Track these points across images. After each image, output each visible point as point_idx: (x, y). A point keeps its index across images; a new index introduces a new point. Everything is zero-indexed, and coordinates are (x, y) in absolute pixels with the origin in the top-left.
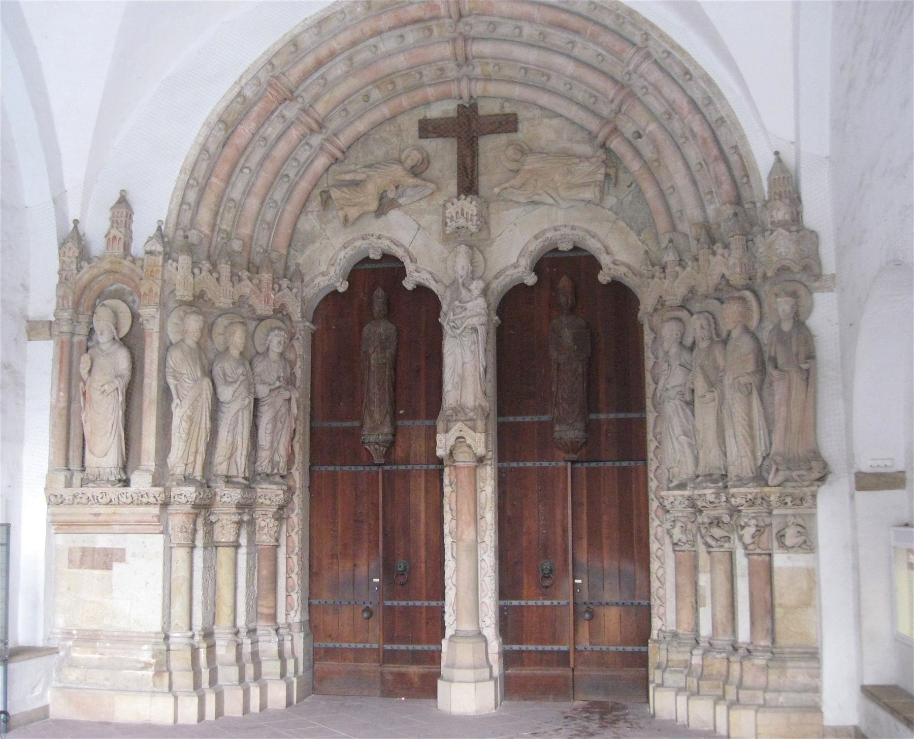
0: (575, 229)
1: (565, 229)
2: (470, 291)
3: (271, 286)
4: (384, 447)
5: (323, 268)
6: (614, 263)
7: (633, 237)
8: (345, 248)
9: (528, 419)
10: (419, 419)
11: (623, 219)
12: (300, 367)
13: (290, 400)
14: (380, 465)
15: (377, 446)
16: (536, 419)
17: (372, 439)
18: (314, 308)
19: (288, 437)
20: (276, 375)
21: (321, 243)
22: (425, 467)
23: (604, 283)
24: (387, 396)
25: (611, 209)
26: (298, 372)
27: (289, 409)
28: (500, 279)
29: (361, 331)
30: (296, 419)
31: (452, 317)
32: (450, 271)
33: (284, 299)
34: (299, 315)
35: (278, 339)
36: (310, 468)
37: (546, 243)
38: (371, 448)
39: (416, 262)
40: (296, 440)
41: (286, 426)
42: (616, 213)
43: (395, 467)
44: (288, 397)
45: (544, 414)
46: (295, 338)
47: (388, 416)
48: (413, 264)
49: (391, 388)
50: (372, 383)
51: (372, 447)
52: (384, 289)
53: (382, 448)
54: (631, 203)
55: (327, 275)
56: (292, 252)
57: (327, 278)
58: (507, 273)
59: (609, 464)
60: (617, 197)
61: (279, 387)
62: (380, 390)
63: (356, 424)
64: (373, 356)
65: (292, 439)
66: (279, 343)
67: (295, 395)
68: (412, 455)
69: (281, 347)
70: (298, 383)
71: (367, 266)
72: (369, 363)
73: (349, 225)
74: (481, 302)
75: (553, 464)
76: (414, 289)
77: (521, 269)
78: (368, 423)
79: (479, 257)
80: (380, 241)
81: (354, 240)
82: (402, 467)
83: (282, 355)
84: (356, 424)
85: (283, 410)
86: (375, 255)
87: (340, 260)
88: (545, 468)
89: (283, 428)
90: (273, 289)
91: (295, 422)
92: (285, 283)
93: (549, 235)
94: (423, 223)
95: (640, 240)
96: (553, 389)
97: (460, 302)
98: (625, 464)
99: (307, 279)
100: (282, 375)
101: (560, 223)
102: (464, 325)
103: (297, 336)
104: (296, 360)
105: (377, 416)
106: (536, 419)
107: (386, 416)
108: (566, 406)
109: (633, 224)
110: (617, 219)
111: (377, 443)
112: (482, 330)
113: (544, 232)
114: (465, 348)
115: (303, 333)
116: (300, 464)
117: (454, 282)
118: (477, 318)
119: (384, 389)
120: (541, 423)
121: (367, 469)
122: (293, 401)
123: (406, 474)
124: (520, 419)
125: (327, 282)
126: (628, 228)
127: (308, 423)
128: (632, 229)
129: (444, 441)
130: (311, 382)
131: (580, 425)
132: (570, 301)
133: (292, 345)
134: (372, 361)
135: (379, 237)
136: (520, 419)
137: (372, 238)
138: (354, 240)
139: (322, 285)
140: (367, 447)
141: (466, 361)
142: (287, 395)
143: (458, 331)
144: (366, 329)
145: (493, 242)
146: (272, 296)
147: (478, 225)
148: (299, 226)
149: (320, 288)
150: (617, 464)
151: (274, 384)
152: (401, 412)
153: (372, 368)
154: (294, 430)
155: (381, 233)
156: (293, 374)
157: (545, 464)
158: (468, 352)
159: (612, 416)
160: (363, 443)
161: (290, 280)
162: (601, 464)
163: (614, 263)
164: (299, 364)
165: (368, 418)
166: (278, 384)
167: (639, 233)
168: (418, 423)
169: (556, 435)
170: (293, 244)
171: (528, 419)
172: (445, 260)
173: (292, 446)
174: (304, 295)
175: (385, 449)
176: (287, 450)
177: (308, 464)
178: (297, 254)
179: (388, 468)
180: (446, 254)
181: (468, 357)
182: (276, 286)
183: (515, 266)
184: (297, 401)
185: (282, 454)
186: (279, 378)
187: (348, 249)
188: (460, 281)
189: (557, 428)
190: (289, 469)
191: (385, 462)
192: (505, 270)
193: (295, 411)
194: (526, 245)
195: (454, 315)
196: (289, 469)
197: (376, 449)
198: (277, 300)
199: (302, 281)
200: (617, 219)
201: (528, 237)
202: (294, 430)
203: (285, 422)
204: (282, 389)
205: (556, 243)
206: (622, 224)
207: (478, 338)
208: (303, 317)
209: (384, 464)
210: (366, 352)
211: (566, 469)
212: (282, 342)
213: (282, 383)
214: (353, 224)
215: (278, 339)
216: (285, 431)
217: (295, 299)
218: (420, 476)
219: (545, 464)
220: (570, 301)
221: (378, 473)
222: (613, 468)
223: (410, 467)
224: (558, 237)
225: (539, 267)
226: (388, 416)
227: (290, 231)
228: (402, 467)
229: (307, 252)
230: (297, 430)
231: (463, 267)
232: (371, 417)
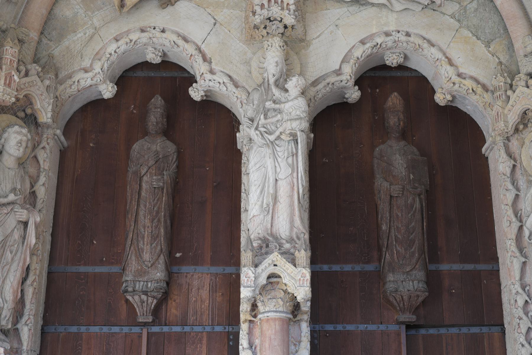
0: (410, 36)
1: (398, 35)
2: (286, 91)
3: (15, 65)
4: (154, 297)
5: (86, 63)
6: (459, 75)
7: (480, 48)
8: (117, 41)
9: (348, 268)
10: (202, 265)
11: (468, 28)
12: (44, 184)
13: (26, 224)
14: (145, 324)
15: (144, 297)
16: (358, 268)
17: (139, 286)
18: (68, 119)
19: (18, 274)
20: (9, 187)
21: (85, 34)
22: (208, 329)
23: (442, 103)
24: (162, 230)
25: (453, 16)
26: (41, 192)
27: (24, 238)
28: (320, 86)
29: (129, 148)
30: (32, 254)
31: (262, 121)
32: (255, 73)
33: (32, 89)
34: (49, 115)
35: (19, 137)
36: (42, 329)
37: (375, 50)
38: (135, 300)
39: (210, 63)
40: (29, 282)
41: (17, 258)
42: (459, 21)
43: (166, 329)
44: (24, 218)
45: (368, 262)
46: (42, 146)
47: (162, 256)
48: (206, 64)
49: (169, 222)
50: (141, 213)
51: (136, 298)
52: (163, 98)
53: (150, 300)
54: (476, 10)
55: (91, 71)
56: (45, 41)
57: (90, 74)
58: (328, 80)
59: (454, 330)
60: (459, 4)
61: (12, 203)
62: (152, 221)
63: (115, 269)
64: (145, 178)
65: (24, 280)
66: (20, 142)
67: (35, 218)
68: (191, 312)
69: (22, 150)
70: (39, 205)
71: (140, 74)
72: (140, 186)
73: (125, 9)
74: (301, 103)
75: (382, 327)
76: (202, 101)
77: (344, 78)
78: (133, 265)
79: (294, 58)
80: (164, 35)
81: (128, 32)
82: (177, 329)
83: (21, 163)
84: (115, 269)
85: (16, 235)
86: (153, 58)
87: (110, 54)
88: (372, 333)
89: (12, 259)
90: (18, 71)
91: (31, 258)
92: (35, 68)
93: (379, 40)
94: (219, 18)
95: (489, 51)
96: (384, 227)
97: (274, 102)
98: (475, 330)
99: (62, 75)
100: (19, 187)
101: (392, 28)
102: (281, 130)
103: (44, 144)
104: (38, 176)
105: (146, 256)
106: (358, 268)
107: (159, 256)
108: (402, 250)
109: (480, 34)
110: (460, 27)
111: (145, 293)
112: (302, 139)
113: (371, 37)
114: (279, 160)
115: (51, 142)
116: (32, 317)
117: (264, 85)
118: (298, 122)
119: (159, 221)
120: (362, 274)
121: (126, 329)
122: (31, 229)
123: (181, 338)
124: (336, 268)
125: (89, 82)
126: (474, 38)
127: (46, 265)
128: (478, 39)
129: (252, 275)
130: (55, 212)
131: (421, 274)
132: (402, 123)
133: (35, 157)
134: (144, 185)
135: (163, 31)
136: (336, 268)
137: (154, 31)
138: (128, 32)
139: (83, 84)
140: (130, 298)
141: (280, 176)
142: (22, 214)
143: (272, 138)
144: (136, 147)
145: (308, 46)
146: (16, 78)
147: (296, 16)
148: (57, 11)
149: (80, 88)
150: (464, 330)
151: (6, 196)
152: (178, 255)
153: (143, 194)
154: (28, 268)
155: (165, 26)
156: (33, 194)
157: (371, 327)
158: (283, 164)
159: (456, 267)
160: (126, 291)
161: (43, 68)
162: (443, 331)
163: (459, 75)
164: (42, 179)
165: (133, 258)
166: (11, 197)
167: (488, 44)
168: (199, 269)
169: (390, 287)
170: (46, 33)
171: (348, 268)
172: (247, 63)
173: (22, 291)
174: (58, 94)
175: (155, 301)
176: (15, 293)
177: (41, 323)
178: (51, 44)
179: (155, 329)
180: (249, 55)
181: (284, 171)
182: (22, 68)
183: (338, 72)
184: (37, 226)
185: (8, 299)
186: (14, 190)
187: (120, 43)
188: (272, 80)
189: (390, 277)
190: (16, 322)
191: (153, 321)
192: (323, 78)
193: (32, 239)
194: (350, 51)
195: (266, 118)
196: (16, 322)
197: (142, 302)
198: (22, 86)
199: (57, 76)
200: (460, 27)
201: (353, 40)
202: (28, 268)
203: (16, 254)
204: (17, 206)
205: (382, 58)
206: (466, 33)
207: (297, 149)
208: (54, 118)
209: (153, 323)
210: (136, 173)
211: (399, 334)
212: (24, 144)
213: (19, 198)
214: (129, 12)
215: (19, 137)
216: (15, 264)
217: (45, 94)
218: (201, 340)
219: (371, 327)
220: (402, 123)
221: (140, 336)
222: (458, 334)
223: (187, 329)
224: (390, 44)
225: (360, 82)
226: (162, 256)
227: (44, 12)
228: (177, 329)
229: (66, 43)
230: (32, 268)
231: (277, 62)
232: (139, 256)
